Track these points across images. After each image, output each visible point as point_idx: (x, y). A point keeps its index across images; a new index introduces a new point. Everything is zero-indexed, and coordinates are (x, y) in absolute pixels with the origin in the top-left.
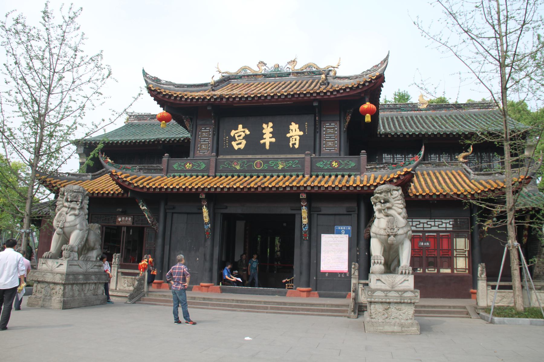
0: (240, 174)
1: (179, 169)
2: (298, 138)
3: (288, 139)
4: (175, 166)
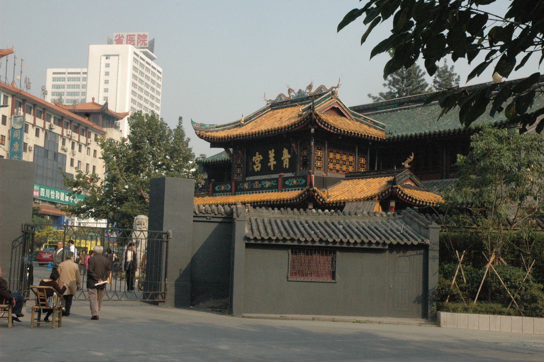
2: (288, 160)
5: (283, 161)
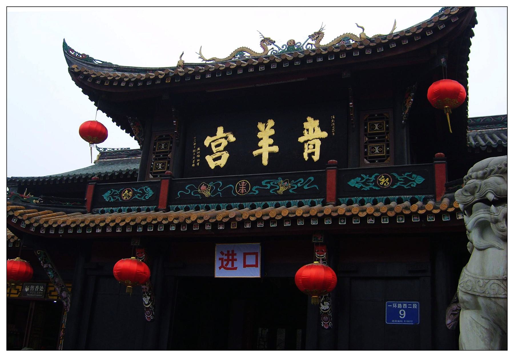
0: (210, 205)
1: (112, 200)
2: (318, 143)
3: (301, 146)
4: (106, 196)
5: (303, 144)
